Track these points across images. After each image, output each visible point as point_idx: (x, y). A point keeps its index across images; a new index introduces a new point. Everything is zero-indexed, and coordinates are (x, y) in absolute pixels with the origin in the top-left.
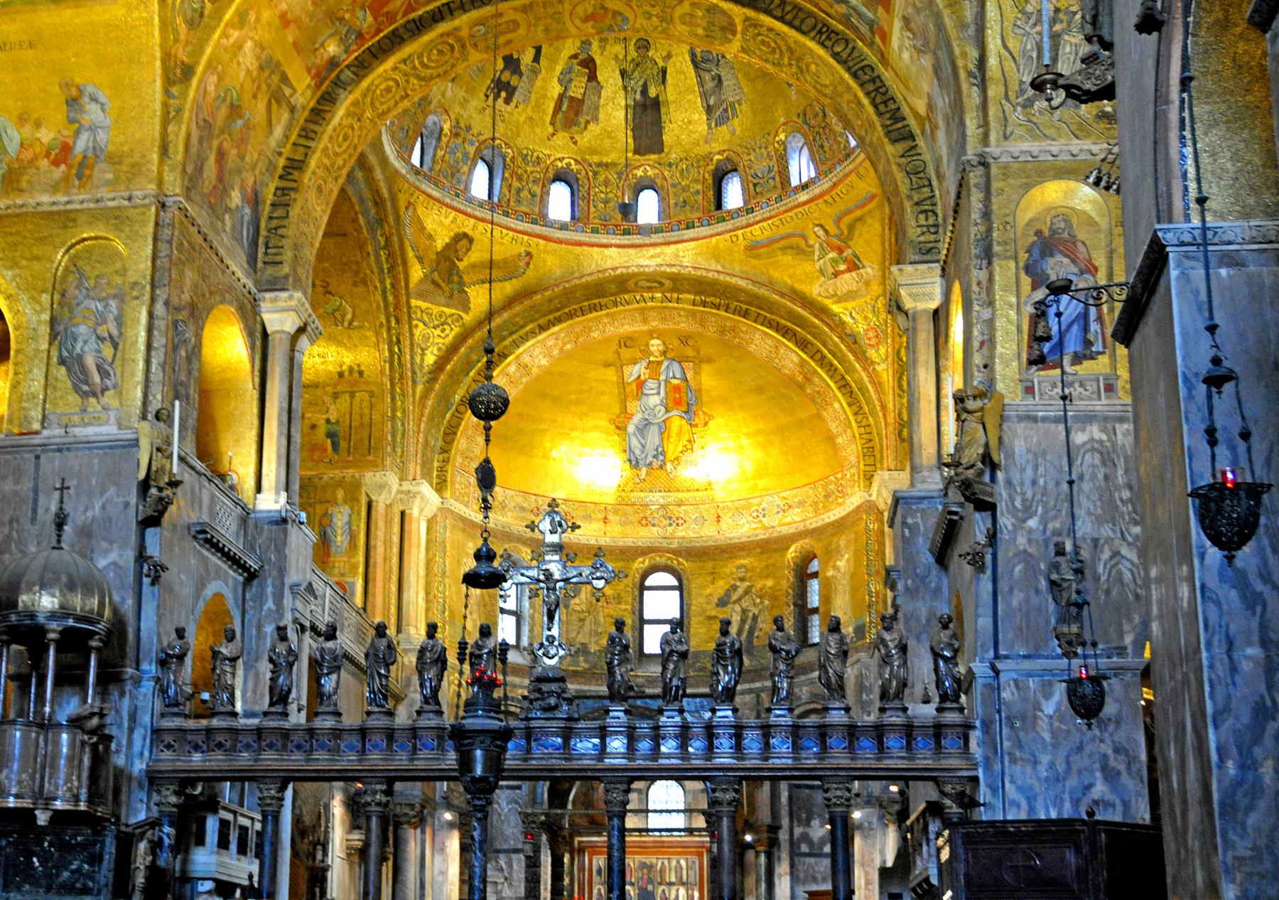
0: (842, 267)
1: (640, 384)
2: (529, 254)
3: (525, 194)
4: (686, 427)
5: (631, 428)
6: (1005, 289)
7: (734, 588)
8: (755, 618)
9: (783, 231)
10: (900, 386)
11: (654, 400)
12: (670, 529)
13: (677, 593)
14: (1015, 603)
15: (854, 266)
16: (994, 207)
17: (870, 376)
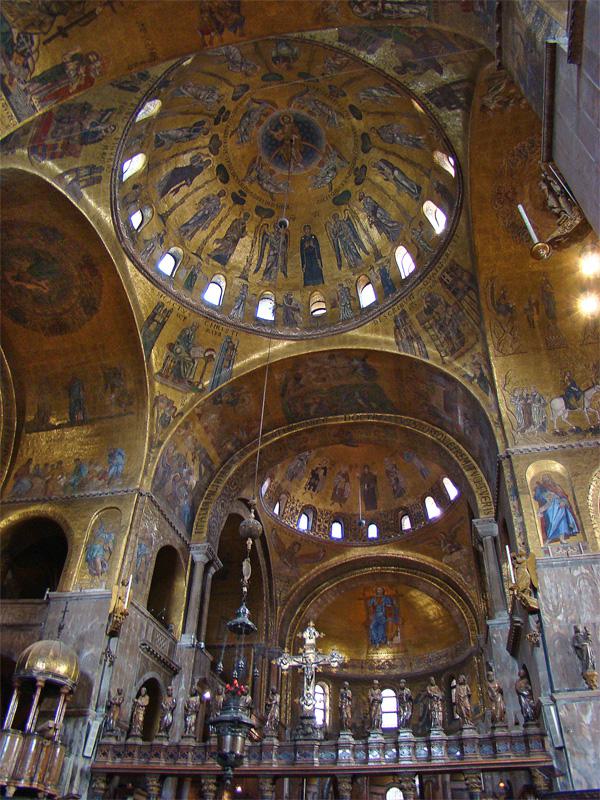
1: (374, 607)
3: (322, 527)
5: (371, 627)
6: (527, 507)
7: (420, 695)
14: (558, 661)
15: (458, 549)
16: (516, 473)
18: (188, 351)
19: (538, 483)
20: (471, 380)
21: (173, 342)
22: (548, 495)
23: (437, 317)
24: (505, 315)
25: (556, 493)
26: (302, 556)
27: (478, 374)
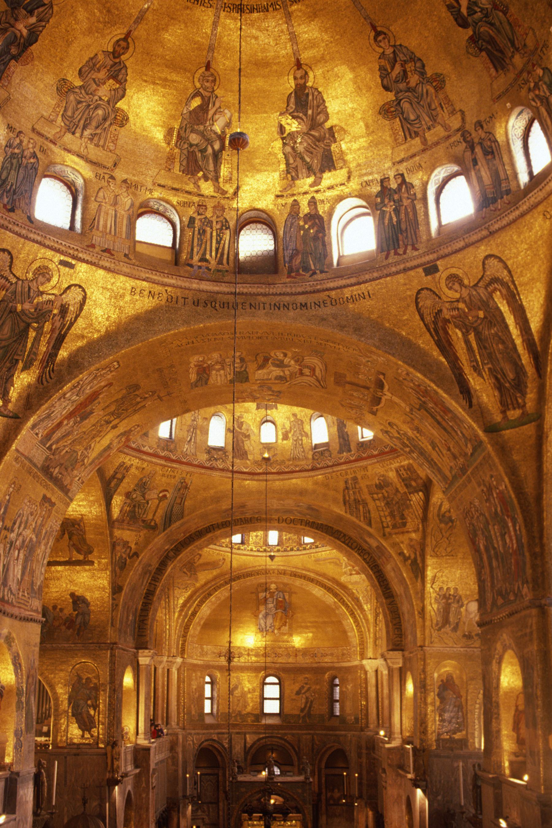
0: (354, 572)
1: (266, 599)
2: (224, 559)
4: (284, 617)
5: (261, 616)
8: (312, 702)
9: (330, 556)
10: (376, 623)
11: (271, 605)
12: (276, 659)
13: (278, 686)
17: (364, 616)
18: (143, 496)
19: (442, 681)
20: (406, 559)
21: (131, 490)
22: (449, 694)
23: (386, 495)
24: (446, 524)
25: (454, 693)
26: (201, 565)
27: (413, 556)
